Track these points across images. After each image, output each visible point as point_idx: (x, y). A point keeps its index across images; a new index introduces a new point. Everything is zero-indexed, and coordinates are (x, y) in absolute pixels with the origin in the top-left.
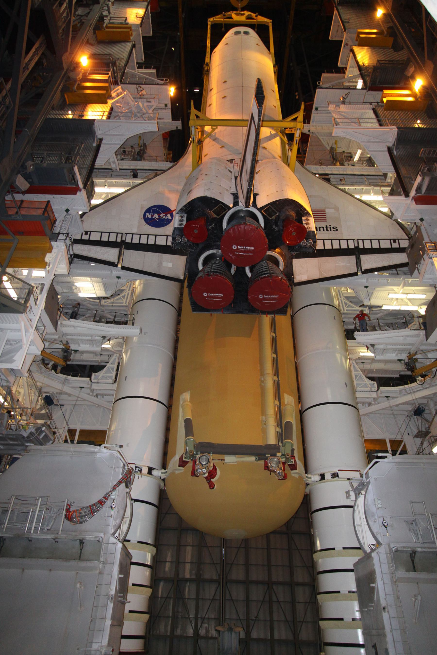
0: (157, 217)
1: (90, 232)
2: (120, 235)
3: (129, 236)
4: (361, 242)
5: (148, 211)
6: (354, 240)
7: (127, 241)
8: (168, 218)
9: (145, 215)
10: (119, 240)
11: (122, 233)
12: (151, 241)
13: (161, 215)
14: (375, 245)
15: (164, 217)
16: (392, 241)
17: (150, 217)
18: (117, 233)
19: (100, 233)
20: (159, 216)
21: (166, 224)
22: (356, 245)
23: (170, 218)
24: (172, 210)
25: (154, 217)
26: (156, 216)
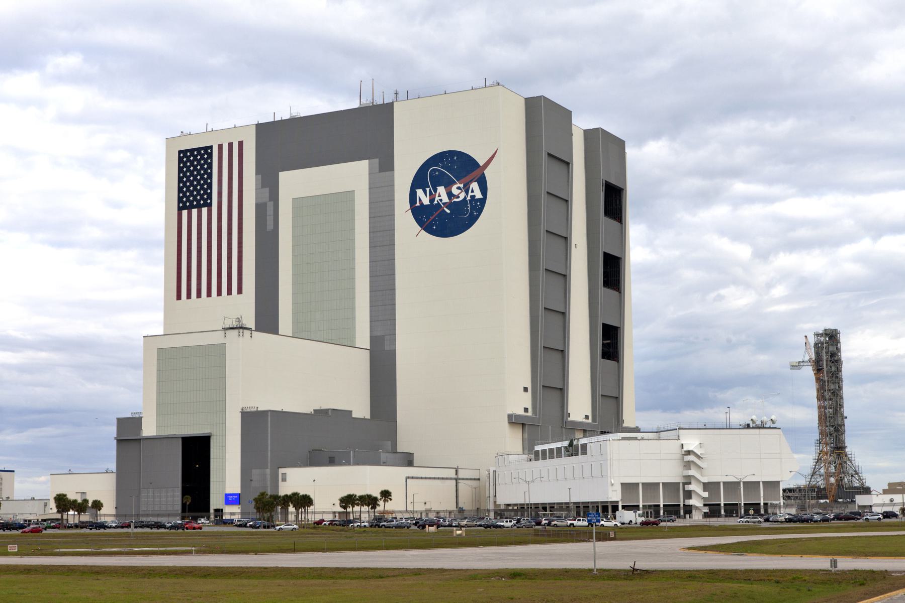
0: (445, 199)
5: (419, 181)
8: (473, 197)
13: (455, 191)
17: (426, 201)
20: (450, 195)
21: (473, 220)
23: (478, 195)
25: (437, 198)
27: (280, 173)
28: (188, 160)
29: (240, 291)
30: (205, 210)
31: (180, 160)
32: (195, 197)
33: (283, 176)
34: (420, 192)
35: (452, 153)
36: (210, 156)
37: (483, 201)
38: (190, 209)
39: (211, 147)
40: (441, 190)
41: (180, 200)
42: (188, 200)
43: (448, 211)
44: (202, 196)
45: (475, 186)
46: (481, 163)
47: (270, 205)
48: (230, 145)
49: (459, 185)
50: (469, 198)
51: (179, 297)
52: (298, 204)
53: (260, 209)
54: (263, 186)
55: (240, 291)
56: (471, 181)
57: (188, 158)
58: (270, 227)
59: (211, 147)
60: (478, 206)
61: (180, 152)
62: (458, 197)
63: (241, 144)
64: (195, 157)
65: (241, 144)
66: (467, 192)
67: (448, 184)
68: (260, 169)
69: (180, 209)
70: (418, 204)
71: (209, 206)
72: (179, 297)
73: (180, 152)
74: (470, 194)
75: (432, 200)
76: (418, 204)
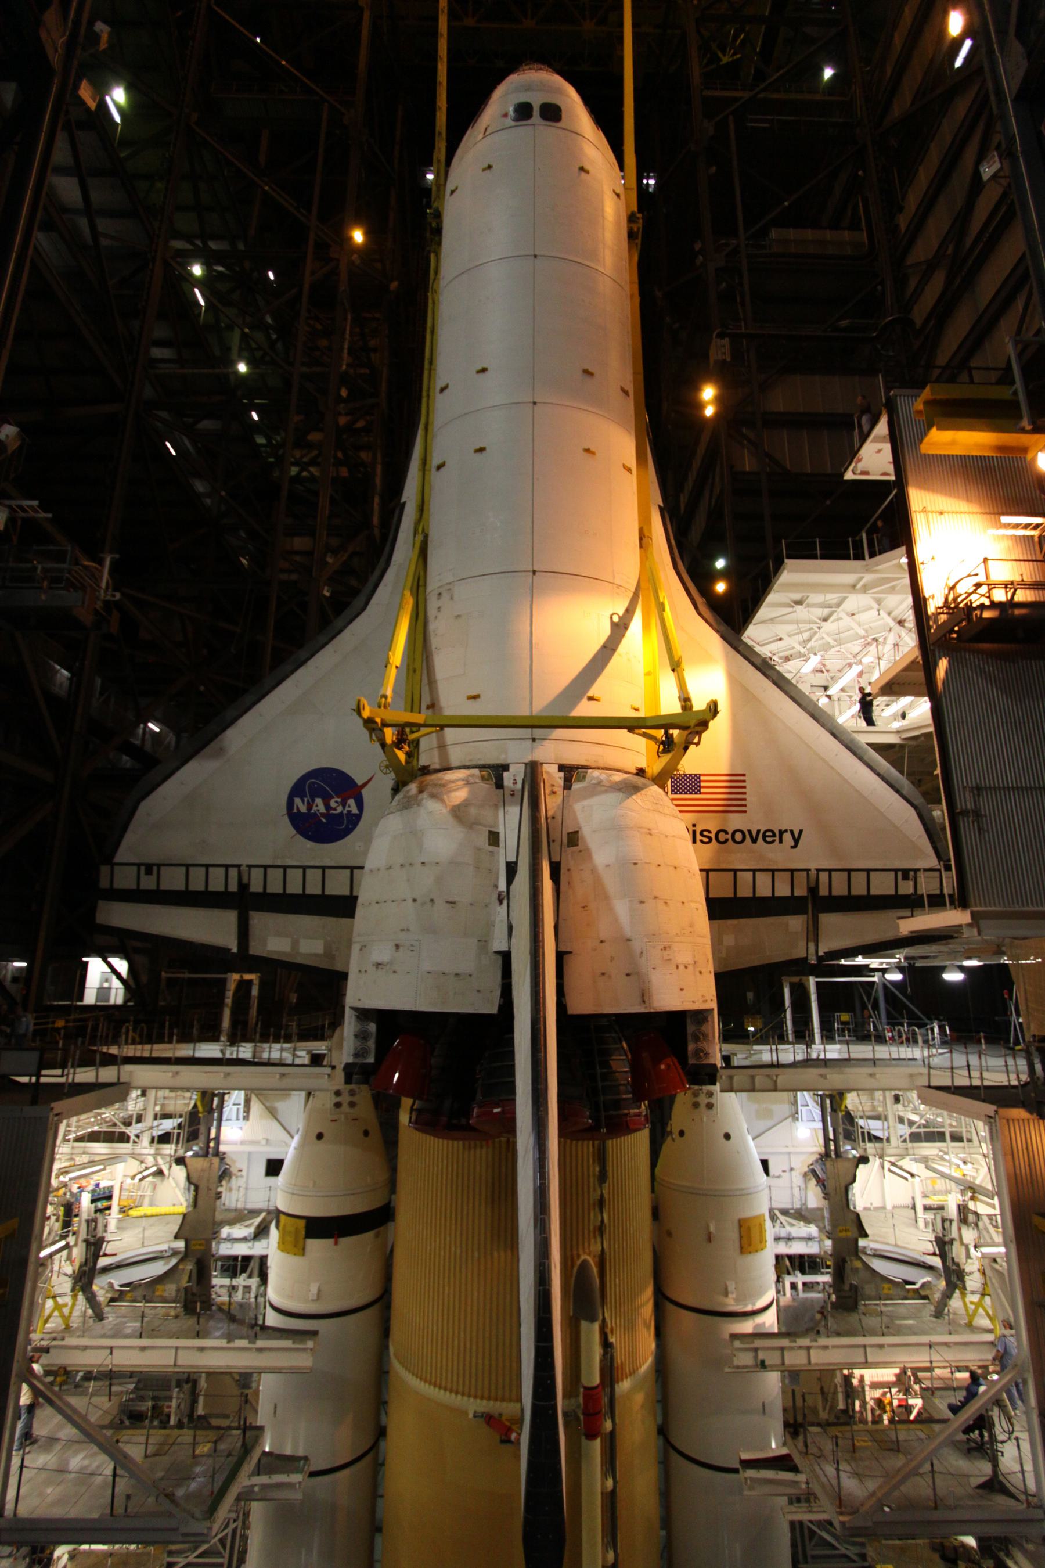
0: (322, 809)
1: (159, 866)
2: (233, 873)
3: (257, 875)
4: (824, 877)
5: (298, 789)
6: (808, 870)
7: (253, 889)
8: (349, 812)
9: (290, 804)
10: (233, 887)
11: (239, 866)
12: (313, 888)
13: (333, 804)
14: (859, 888)
15: (340, 809)
16: (900, 874)
17: (303, 809)
18: (227, 867)
19: (184, 869)
21: (348, 832)
22: (813, 884)
23: (355, 811)
24: (360, 782)
25: (314, 808)
26: (319, 805)
34: (297, 801)
37: (359, 817)
40: (319, 801)
43: (324, 821)
45: (351, 802)
46: (360, 783)
49: (336, 799)
50: (345, 812)
56: (349, 798)
60: (354, 821)
62: (335, 809)
66: (344, 807)
70: (295, 811)
74: (347, 808)
75: (309, 808)
76: (295, 811)
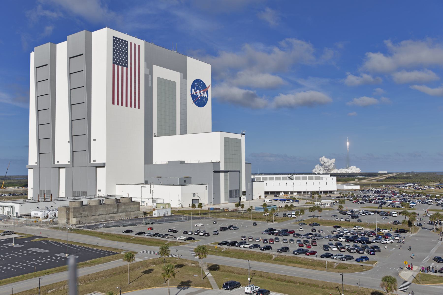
0: (199, 95)
5: (193, 87)
17: (195, 94)
23: (206, 97)
27: (153, 65)
28: (117, 42)
29: (139, 108)
30: (125, 68)
31: (114, 41)
32: (120, 61)
33: (155, 67)
34: (193, 90)
35: (201, 81)
36: (127, 45)
37: (207, 98)
38: (118, 65)
39: (127, 42)
40: (198, 91)
41: (114, 59)
42: (117, 61)
44: (123, 62)
45: (205, 93)
47: (150, 76)
48: (135, 45)
51: (113, 103)
52: (160, 80)
53: (146, 76)
54: (147, 68)
55: (139, 108)
57: (117, 42)
58: (150, 85)
59: (127, 42)
61: (114, 37)
63: (139, 46)
64: (120, 43)
65: (139, 46)
67: (200, 90)
68: (146, 60)
69: (114, 63)
71: (127, 67)
72: (113, 103)
73: (114, 37)
75: (196, 94)
